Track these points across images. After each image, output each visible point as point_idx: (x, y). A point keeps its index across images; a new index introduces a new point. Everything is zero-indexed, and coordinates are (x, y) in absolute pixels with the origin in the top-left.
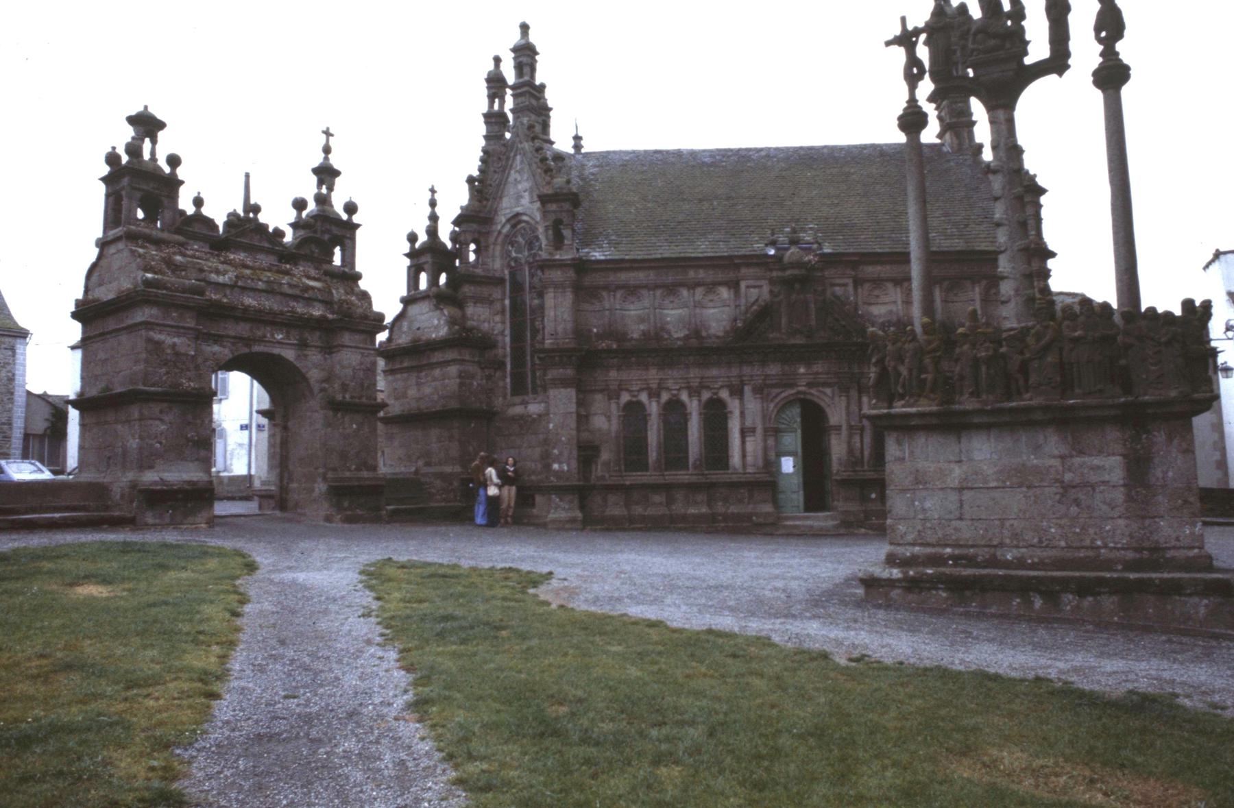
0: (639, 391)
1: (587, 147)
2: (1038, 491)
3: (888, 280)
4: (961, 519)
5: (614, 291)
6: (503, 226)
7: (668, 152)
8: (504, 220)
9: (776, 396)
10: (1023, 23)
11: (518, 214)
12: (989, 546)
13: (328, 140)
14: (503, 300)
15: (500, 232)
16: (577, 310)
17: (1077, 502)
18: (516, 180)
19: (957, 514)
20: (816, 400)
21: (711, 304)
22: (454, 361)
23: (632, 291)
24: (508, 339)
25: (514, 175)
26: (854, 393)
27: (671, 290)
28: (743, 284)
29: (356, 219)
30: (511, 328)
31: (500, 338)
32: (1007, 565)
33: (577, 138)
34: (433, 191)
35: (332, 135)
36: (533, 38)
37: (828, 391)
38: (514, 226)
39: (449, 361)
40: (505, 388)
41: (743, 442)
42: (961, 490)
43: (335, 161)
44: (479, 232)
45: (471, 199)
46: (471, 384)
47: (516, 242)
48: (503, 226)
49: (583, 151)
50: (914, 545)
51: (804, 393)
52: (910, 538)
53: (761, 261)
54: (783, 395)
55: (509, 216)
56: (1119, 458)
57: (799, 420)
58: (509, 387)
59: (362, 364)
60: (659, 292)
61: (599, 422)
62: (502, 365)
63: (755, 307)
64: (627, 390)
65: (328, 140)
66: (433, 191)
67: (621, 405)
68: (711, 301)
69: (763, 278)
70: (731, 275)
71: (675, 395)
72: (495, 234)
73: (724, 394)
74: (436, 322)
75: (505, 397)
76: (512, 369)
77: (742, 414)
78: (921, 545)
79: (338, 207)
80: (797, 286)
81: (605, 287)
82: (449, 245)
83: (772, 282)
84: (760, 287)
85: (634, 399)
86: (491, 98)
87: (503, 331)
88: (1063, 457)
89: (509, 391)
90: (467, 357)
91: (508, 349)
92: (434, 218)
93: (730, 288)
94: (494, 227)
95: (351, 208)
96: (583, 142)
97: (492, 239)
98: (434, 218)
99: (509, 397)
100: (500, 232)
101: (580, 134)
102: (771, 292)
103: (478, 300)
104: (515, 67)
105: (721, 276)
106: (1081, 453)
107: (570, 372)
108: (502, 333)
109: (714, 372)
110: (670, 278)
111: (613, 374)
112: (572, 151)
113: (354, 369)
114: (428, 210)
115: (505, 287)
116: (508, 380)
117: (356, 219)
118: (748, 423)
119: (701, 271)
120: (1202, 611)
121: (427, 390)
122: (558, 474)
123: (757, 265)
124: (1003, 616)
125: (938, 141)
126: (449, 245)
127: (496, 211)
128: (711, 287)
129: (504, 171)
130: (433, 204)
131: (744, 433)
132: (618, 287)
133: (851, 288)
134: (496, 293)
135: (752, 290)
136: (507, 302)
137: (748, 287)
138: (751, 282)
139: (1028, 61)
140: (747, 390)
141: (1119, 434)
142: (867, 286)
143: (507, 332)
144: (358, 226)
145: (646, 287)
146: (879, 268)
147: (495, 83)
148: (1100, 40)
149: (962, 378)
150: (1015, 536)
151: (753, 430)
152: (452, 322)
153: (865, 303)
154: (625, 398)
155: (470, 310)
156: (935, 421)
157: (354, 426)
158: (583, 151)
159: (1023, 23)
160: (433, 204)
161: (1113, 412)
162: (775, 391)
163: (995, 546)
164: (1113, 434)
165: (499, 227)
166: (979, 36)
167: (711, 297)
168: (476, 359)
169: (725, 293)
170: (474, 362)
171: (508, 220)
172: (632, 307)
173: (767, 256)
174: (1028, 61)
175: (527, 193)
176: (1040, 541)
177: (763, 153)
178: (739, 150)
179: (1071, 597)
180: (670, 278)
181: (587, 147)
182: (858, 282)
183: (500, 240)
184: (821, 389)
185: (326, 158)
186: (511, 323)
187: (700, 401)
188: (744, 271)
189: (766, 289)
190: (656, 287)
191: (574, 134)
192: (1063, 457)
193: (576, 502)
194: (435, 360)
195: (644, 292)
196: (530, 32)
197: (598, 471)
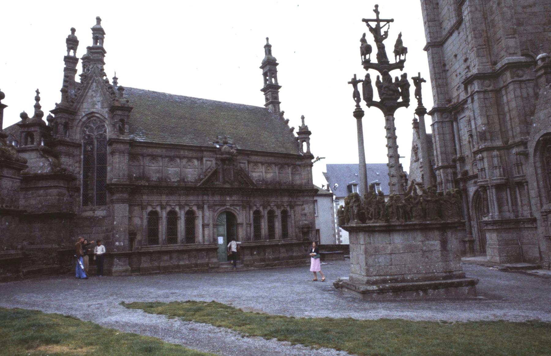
0: (156, 206)
2: (415, 254)
4: (391, 265)
6: (83, 118)
7: (159, 93)
8: (84, 114)
9: (217, 210)
11: (93, 112)
12: (401, 274)
14: (80, 155)
15: (80, 120)
17: (427, 257)
18: (92, 95)
19: (390, 263)
20: (233, 212)
21: (189, 167)
22: (55, 187)
23: (154, 157)
24: (82, 176)
25: (90, 93)
26: (248, 209)
27: (172, 159)
28: (204, 159)
30: (84, 170)
31: (78, 175)
32: (408, 281)
33: (115, 79)
34: (38, 92)
36: (103, 25)
37: (238, 208)
38: (89, 118)
39: (51, 187)
40: (80, 202)
41: (203, 230)
42: (391, 254)
44: (69, 119)
45: (62, 100)
46: (63, 199)
47: (90, 126)
48: (83, 118)
50: (375, 276)
51: (228, 209)
52: (375, 273)
53: (213, 150)
54: (220, 210)
55: (87, 113)
56: (439, 241)
57: (225, 220)
58: (81, 201)
59: (12, 187)
60: (167, 159)
61: (137, 221)
62: (78, 190)
64: (151, 205)
66: (38, 92)
67: (148, 213)
68: (189, 165)
69: (212, 157)
70: (199, 155)
71: (173, 208)
72: (78, 121)
73: (195, 208)
74: (41, 164)
75: (79, 207)
76: (83, 192)
77: (203, 217)
78: (378, 276)
80: (227, 162)
82: (47, 123)
83: (217, 159)
84: (211, 161)
85: (154, 210)
86: (69, 49)
87: (79, 172)
88: (422, 241)
89: (81, 204)
90: (62, 185)
91: (82, 182)
92: (37, 107)
93: (198, 160)
94: (77, 117)
96: (118, 81)
97: (75, 123)
98: (37, 107)
99: (81, 206)
100: (80, 120)
101: (117, 77)
102: (216, 164)
103: (68, 155)
104: (93, 38)
105: (195, 155)
106: (428, 240)
107: (125, 196)
108: (79, 173)
109: (191, 198)
110: (172, 154)
113: (8, 190)
114: (34, 102)
115: (81, 149)
116: (81, 197)
118: (206, 222)
119: (186, 151)
120: (467, 291)
121: (33, 202)
122: (118, 247)
123: (210, 151)
124: (410, 301)
125: (264, 107)
126: (47, 123)
127: (79, 109)
128: (190, 159)
129: (85, 89)
130: (37, 99)
131: (204, 226)
133: (247, 165)
134: (76, 152)
135: (208, 162)
136: (82, 157)
137: (207, 161)
138: (208, 159)
140: (206, 206)
141: (438, 233)
142: (252, 164)
143: (82, 172)
144: (5, 106)
145: (161, 156)
146: (256, 157)
147: (72, 42)
148: (417, 99)
149: (393, 213)
150: (409, 270)
152: (53, 166)
154: (150, 209)
155: (64, 159)
156: (384, 229)
157: (7, 223)
158: (118, 85)
160: (37, 99)
161: (439, 226)
162: (218, 207)
163: (403, 274)
164: (437, 233)
165: (80, 118)
166: (386, 89)
168: (66, 186)
169: (196, 162)
170: (65, 187)
171: (86, 115)
173: (216, 148)
175: (100, 103)
176: (417, 272)
177: (201, 101)
178: (191, 98)
179: (431, 290)
180: (172, 154)
182: (249, 162)
183: (81, 123)
184: (235, 207)
186: (84, 168)
188: (205, 153)
189: (214, 162)
190: (166, 157)
191: (114, 76)
192: (422, 241)
193: (127, 261)
194: (40, 185)
195: (160, 159)
196: (101, 22)
197: (136, 245)
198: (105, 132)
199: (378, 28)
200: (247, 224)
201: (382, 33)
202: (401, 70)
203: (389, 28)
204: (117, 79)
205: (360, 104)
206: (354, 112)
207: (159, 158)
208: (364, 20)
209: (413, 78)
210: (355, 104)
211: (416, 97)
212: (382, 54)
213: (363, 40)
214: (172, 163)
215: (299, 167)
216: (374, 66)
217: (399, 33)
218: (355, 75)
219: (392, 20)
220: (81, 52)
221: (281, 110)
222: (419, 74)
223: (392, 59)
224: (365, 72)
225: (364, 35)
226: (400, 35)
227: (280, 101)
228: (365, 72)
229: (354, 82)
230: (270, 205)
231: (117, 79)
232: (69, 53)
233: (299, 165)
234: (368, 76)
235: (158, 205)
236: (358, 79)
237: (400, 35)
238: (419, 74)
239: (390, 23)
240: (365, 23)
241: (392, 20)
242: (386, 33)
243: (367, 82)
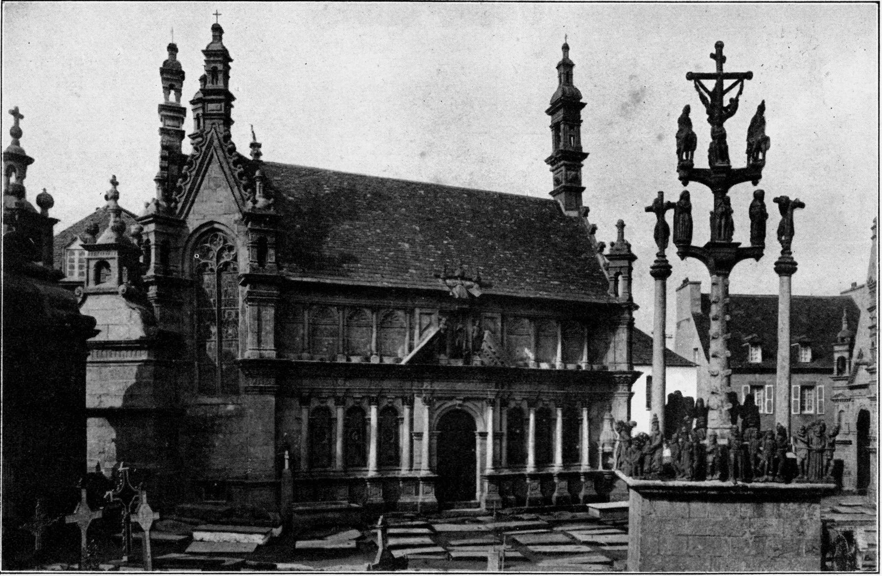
13: (17, 123)
20: (471, 412)
29: (52, 213)
33: (255, 146)
35: (22, 117)
37: (479, 405)
43: (27, 146)
65: (17, 123)
79: (31, 198)
86: (167, 89)
95: (46, 201)
96: (262, 150)
101: (258, 141)
111: (306, 382)
117: (52, 213)
118: (416, 430)
151: (420, 435)
185: (17, 143)
191: (252, 140)
198: (235, 259)
199: (719, 92)
201: (726, 103)
203: (740, 93)
204: (259, 146)
205: (667, 251)
210: (657, 249)
212: (719, 149)
213: (685, 121)
217: (760, 103)
218: (661, 194)
219: (749, 76)
220: (191, 88)
223: (738, 159)
224: (680, 188)
227: (583, 185)
228: (680, 188)
229: (659, 207)
231: (259, 146)
232: (167, 98)
234: (685, 196)
236: (665, 200)
239: (745, 81)
241: (749, 76)
242: (734, 103)
243: (684, 207)
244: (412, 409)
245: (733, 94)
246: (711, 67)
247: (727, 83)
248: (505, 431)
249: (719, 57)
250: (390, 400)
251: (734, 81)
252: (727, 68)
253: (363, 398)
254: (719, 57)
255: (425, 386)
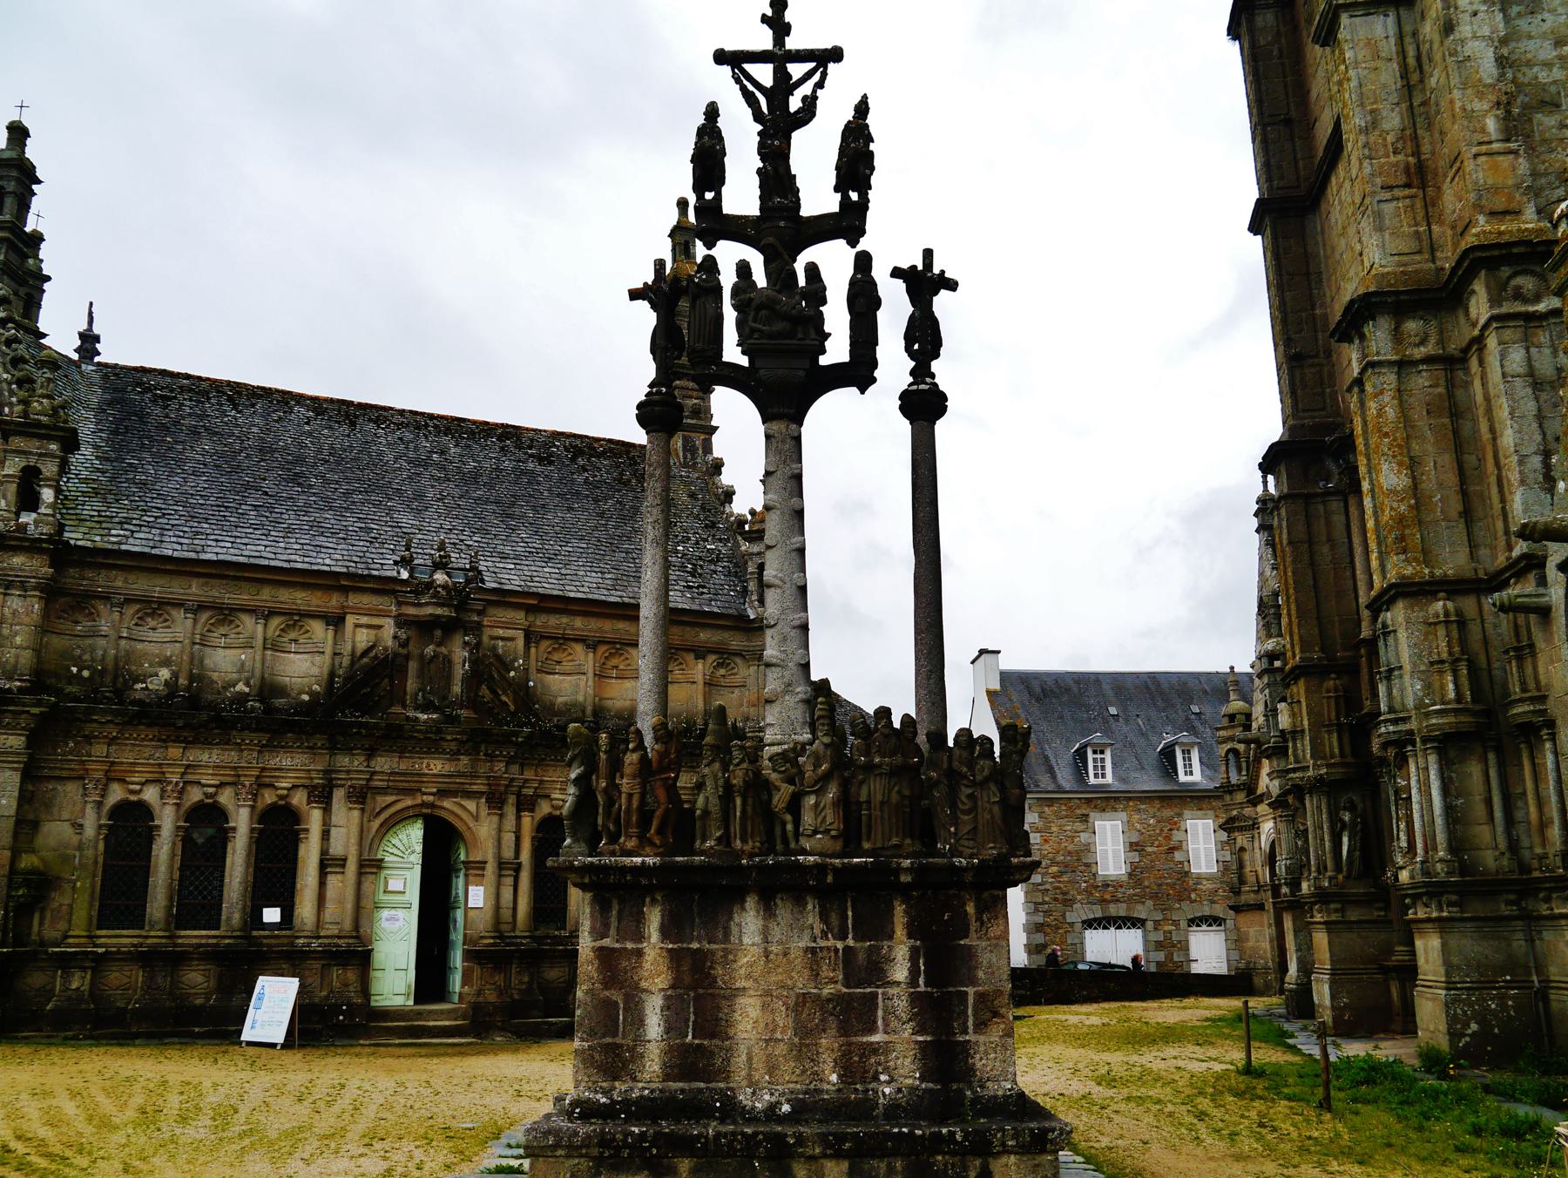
0: (143, 784)
1: (109, 353)
3: (577, 640)
5: (121, 605)
9: (383, 809)
10: (913, 364)
16: (45, 627)
20: (451, 819)
21: (293, 647)
23: (155, 608)
26: (510, 811)
27: (225, 614)
28: (350, 620)
33: (89, 340)
36: (32, 152)
37: (471, 805)
41: (322, 884)
49: (97, 359)
51: (432, 805)
53: (386, 587)
54: (399, 806)
57: (419, 848)
61: (56, 832)
63: (365, 660)
64: (122, 781)
70: (334, 602)
73: (299, 799)
77: (326, 835)
81: (106, 598)
83: (402, 621)
84: (380, 627)
85: (133, 798)
102: (395, 637)
109: (284, 760)
112: (75, 356)
118: (336, 848)
132: (129, 601)
133: (521, 643)
137: (357, 626)
138: (364, 620)
139: (824, 360)
140: (339, 795)
142: (545, 644)
146: (565, 620)
151: (342, 862)
153: (539, 671)
154: (116, 794)
158: (97, 359)
159: (913, 364)
167: (293, 635)
169: (318, 628)
172: (152, 636)
174: (824, 360)
181: (109, 353)
182: (530, 637)
187: (253, 807)
188: (354, 600)
190: (201, 607)
195: (179, 614)
199: (784, 85)
200: (501, 865)
202: (853, 244)
204: (97, 339)
206: (639, 407)
207: (174, 613)
208: (721, 57)
209: (897, 273)
211: (908, 349)
214: (223, 630)
215: (738, 660)
216: (737, 229)
219: (836, 55)
221: (717, 453)
222: (928, 254)
225: (712, 112)
226: (862, 108)
230: (547, 797)
233: (739, 654)
235: (222, 785)
237: (862, 108)
238: (928, 254)
239: (831, 66)
240: (726, 70)
241: (836, 55)
242: (810, 104)
244: (327, 811)
245: (806, 88)
246: (763, 39)
247: (796, 70)
248: (525, 856)
249: (778, 24)
250: (280, 792)
251: (812, 65)
252: (792, 43)
253: (222, 785)
254: (778, 24)
255: (356, 763)
